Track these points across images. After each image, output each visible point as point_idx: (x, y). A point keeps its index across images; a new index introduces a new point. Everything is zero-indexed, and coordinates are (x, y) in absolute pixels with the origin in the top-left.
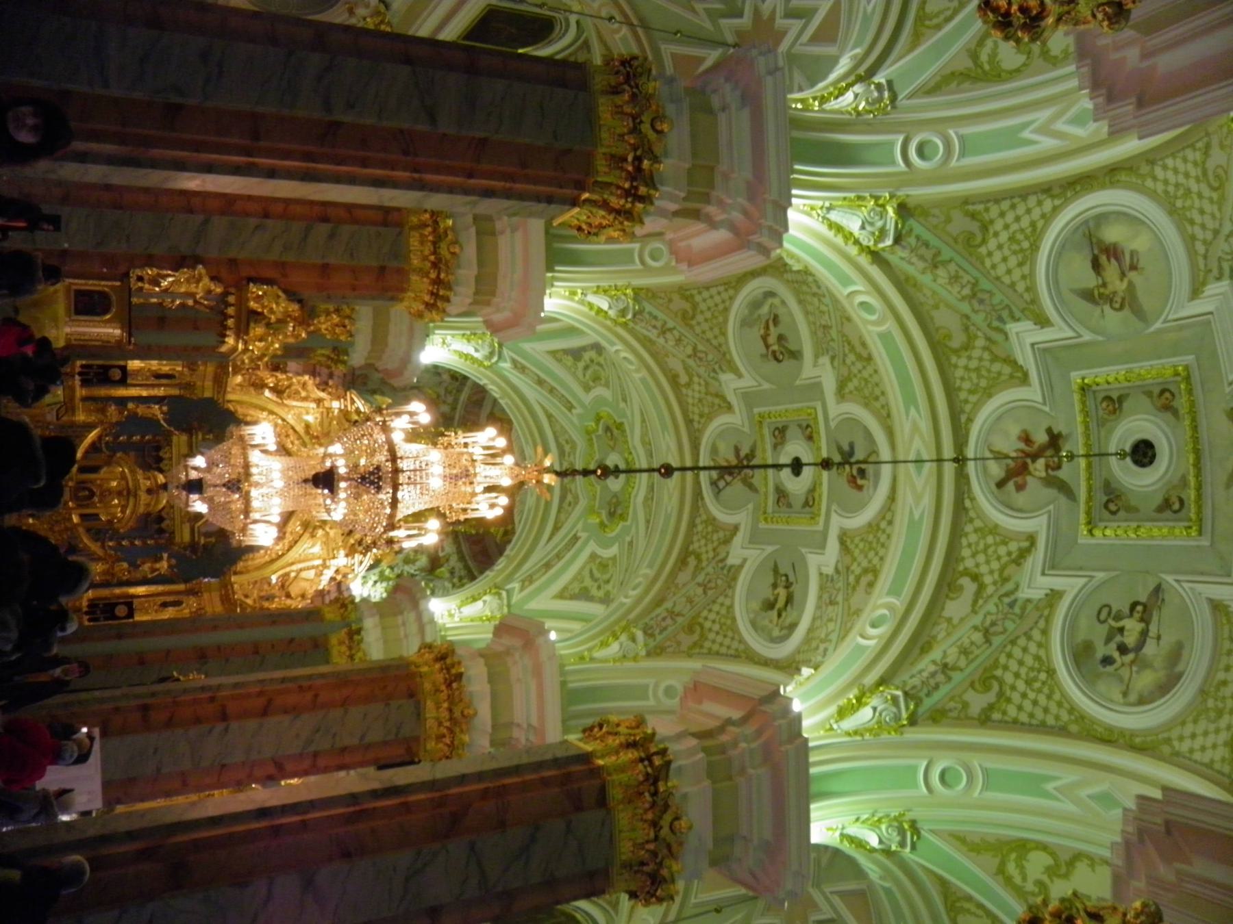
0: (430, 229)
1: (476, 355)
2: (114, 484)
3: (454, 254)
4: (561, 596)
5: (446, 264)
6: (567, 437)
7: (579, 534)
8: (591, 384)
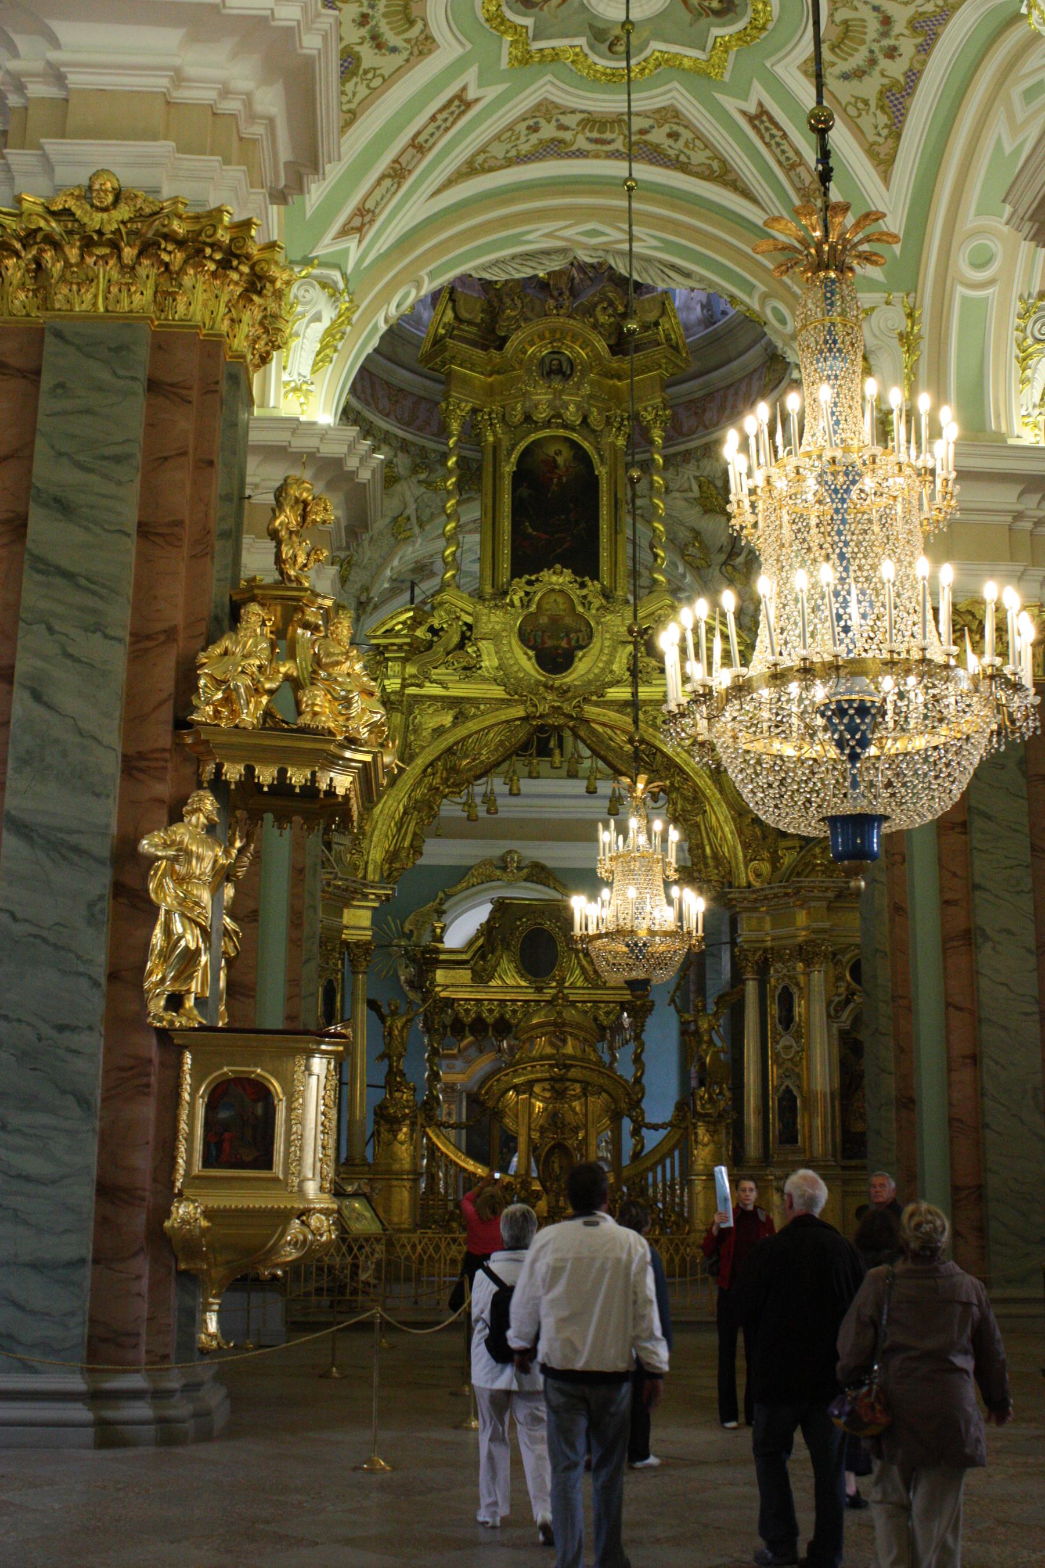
0: (48, 255)
1: (326, 323)
2: (539, 1105)
3: (118, 195)
4: (884, 163)
5: (140, 216)
6: (522, 127)
7: (752, 109)
8: (415, 32)
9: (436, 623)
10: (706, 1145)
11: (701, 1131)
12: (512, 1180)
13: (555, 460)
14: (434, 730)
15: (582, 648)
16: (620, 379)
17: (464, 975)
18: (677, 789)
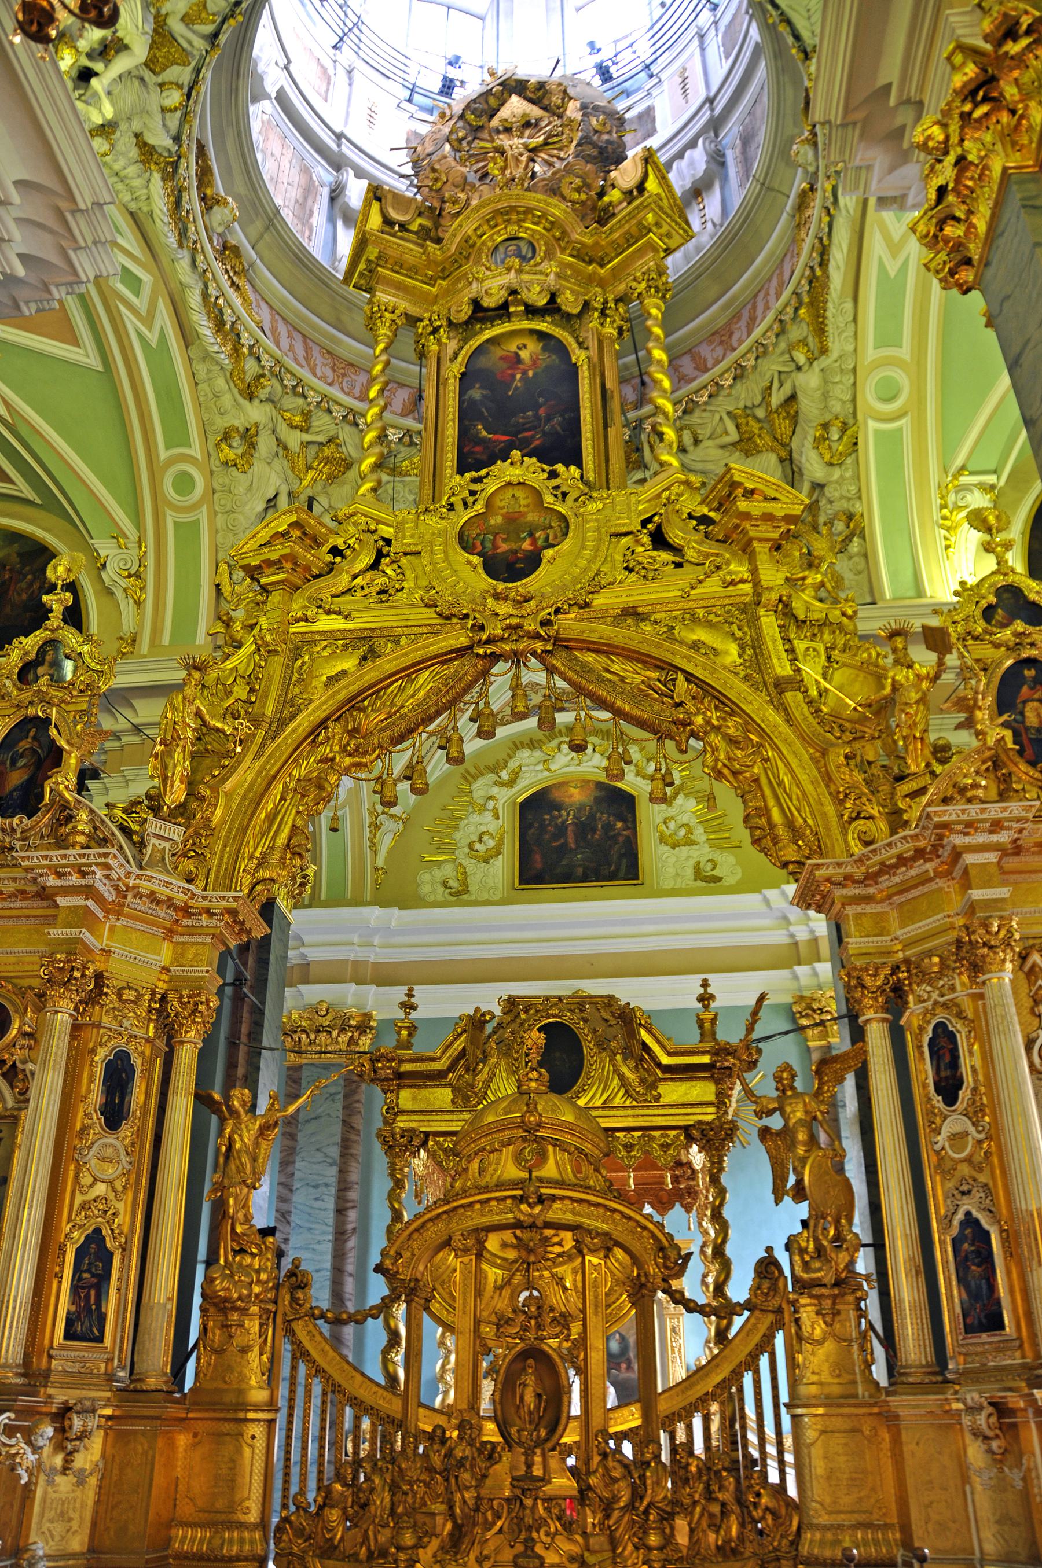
9: (340, 542)
10: (821, 1343)
11: (807, 1314)
12: (441, 1420)
13: (517, 355)
14: (330, 679)
15: (553, 546)
16: (602, 266)
17: (443, 1096)
18: (717, 729)
